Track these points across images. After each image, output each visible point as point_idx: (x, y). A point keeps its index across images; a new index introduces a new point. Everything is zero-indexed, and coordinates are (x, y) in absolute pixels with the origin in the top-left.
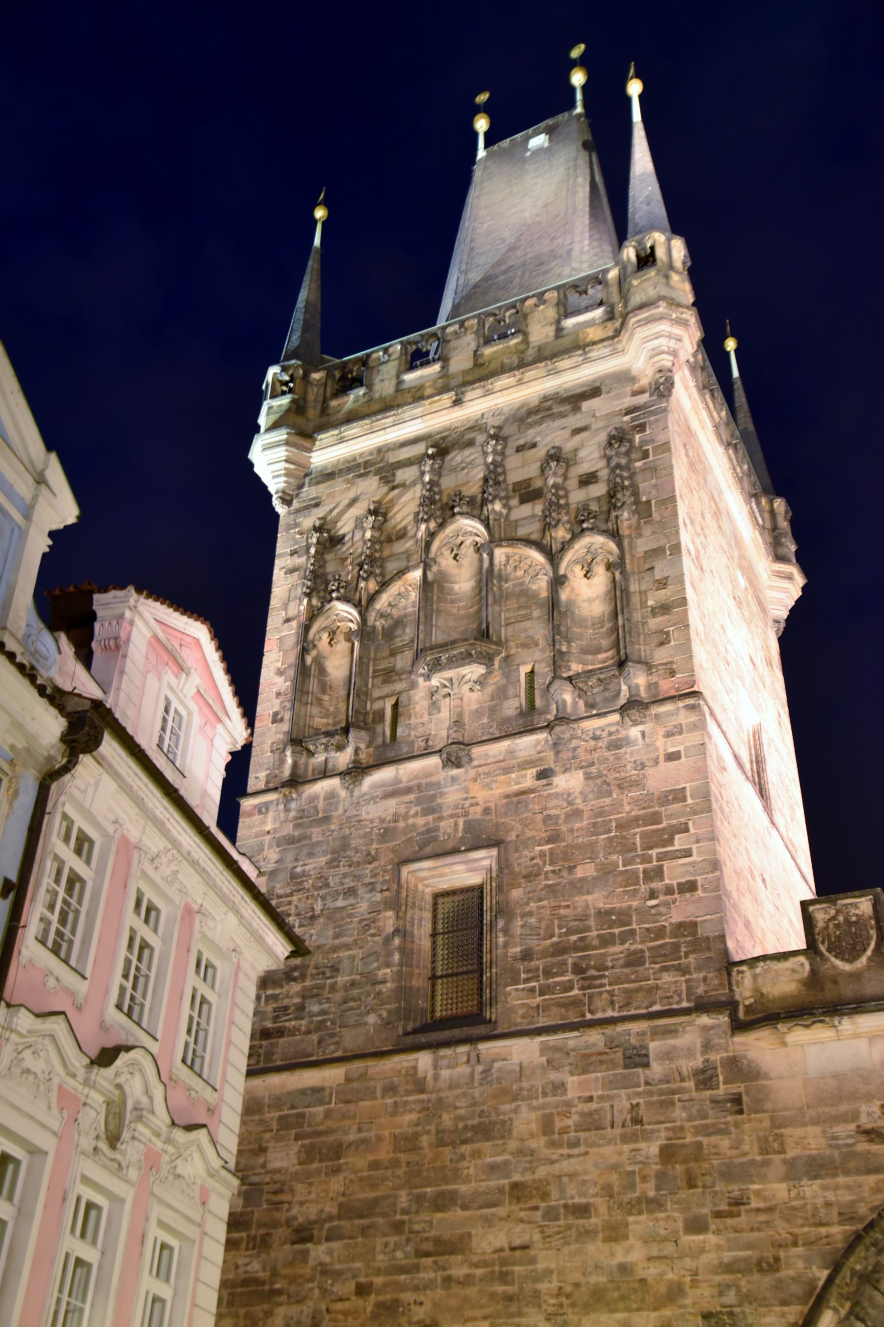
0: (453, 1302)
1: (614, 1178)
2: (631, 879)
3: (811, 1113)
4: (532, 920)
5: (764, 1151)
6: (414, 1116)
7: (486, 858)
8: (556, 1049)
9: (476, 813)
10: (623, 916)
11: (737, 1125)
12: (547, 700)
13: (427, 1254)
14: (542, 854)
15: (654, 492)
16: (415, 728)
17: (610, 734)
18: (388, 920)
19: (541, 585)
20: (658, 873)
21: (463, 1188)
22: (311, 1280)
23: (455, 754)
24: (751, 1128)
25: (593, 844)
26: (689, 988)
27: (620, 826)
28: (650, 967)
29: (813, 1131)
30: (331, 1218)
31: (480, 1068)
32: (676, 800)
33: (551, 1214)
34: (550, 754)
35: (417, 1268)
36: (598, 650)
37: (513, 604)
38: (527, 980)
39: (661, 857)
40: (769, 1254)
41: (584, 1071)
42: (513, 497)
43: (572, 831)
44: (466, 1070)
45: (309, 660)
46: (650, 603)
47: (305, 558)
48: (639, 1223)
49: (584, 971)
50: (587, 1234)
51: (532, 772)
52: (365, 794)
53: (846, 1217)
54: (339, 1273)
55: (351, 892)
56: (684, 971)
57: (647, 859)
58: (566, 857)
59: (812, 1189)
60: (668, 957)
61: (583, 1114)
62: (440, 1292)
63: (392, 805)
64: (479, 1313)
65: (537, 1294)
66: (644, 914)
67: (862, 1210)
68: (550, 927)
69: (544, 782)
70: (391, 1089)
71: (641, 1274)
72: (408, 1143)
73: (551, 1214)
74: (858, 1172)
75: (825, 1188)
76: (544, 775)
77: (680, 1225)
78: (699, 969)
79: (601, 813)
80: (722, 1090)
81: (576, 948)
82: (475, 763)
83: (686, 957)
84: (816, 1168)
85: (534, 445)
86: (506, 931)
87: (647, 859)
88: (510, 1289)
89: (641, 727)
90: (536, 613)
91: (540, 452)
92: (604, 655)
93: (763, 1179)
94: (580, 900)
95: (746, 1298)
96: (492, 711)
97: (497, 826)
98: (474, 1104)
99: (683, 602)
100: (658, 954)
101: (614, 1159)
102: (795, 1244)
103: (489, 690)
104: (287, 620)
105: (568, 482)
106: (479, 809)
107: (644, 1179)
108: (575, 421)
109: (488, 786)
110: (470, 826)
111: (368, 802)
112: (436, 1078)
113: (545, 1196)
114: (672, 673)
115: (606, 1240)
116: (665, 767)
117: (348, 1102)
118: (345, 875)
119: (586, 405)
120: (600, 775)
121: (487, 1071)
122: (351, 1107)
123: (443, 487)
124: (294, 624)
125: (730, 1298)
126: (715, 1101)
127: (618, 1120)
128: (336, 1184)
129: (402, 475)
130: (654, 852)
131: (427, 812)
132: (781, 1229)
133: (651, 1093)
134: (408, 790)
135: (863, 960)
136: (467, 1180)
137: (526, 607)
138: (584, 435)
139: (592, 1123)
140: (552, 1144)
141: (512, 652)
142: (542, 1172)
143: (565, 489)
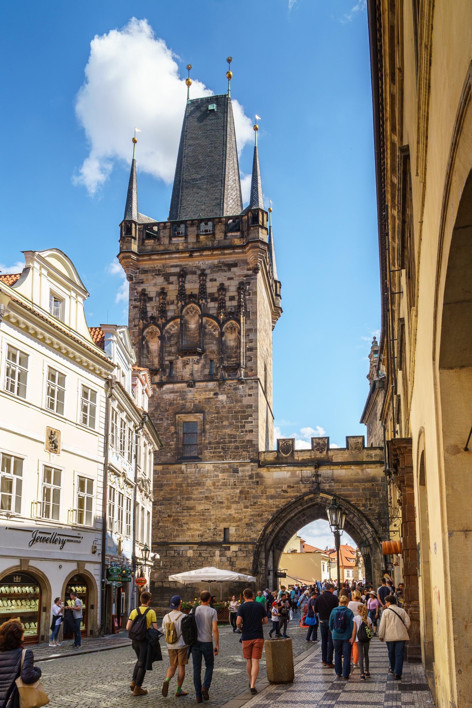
0: (191, 519)
1: (229, 496)
2: (237, 427)
3: (273, 486)
4: (212, 434)
5: (262, 493)
6: (181, 479)
7: (200, 416)
8: (217, 467)
9: (197, 402)
10: (235, 437)
11: (257, 487)
12: (217, 371)
13: (185, 510)
14: (215, 417)
15: (251, 309)
16: (178, 373)
17: (234, 385)
18: (172, 429)
19: (216, 333)
20: (244, 426)
21: (194, 496)
22: (157, 513)
23: (191, 384)
24: (260, 488)
25: (228, 416)
26: (249, 456)
27: (235, 412)
28: (240, 450)
29: (273, 490)
30: (161, 501)
31: (198, 470)
32: (250, 408)
33: (214, 503)
34: (218, 388)
35: (183, 512)
36: (232, 357)
37: (207, 337)
38: (210, 449)
39: (245, 422)
40: (261, 513)
41: (223, 473)
42: (209, 299)
43: (223, 412)
44: (195, 470)
45: (144, 343)
46: (247, 347)
47: (139, 303)
48: (234, 506)
49: (224, 449)
50: (222, 508)
51: (212, 393)
52: (164, 391)
53: (277, 507)
54: (164, 512)
55: (161, 419)
56: (249, 452)
57: (241, 422)
58: (221, 418)
59: (271, 501)
60: (245, 448)
61: (222, 482)
62: (188, 518)
63: (172, 396)
64: (198, 522)
65: (211, 519)
66: (239, 437)
67: (280, 506)
68: (216, 437)
69: (216, 396)
70: (175, 472)
71: (234, 516)
72: (180, 485)
73: (214, 503)
74: (281, 498)
75: (273, 501)
76: (216, 394)
77: (243, 507)
78: (252, 452)
79: (230, 408)
80: (254, 480)
81: (223, 443)
82: (196, 387)
83: (249, 448)
84: (272, 497)
85: (215, 280)
86: (204, 436)
87: (241, 422)
88: (204, 518)
89: (242, 385)
90: (215, 342)
91: (217, 284)
92: (233, 359)
93: (261, 499)
94: (224, 431)
95: (255, 521)
96: (202, 371)
97: (203, 407)
98: (196, 478)
99: (256, 348)
100: (243, 447)
101: (229, 493)
102: (266, 511)
103: (200, 365)
104: (135, 326)
105: (226, 298)
106: (197, 401)
107: (236, 497)
108: (229, 274)
109: (200, 395)
110: (195, 405)
111: (165, 393)
112: (186, 471)
113: (213, 499)
114: (252, 370)
115: (226, 509)
116: (248, 398)
117: (164, 474)
118: (159, 414)
119: (233, 269)
120: (231, 397)
121: (200, 470)
122: (164, 476)
123: (186, 288)
124: (137, 327)
125: (252, 521)
126: (253, 482)
127: (231, 484)
128: (162, 493)
129: (173, 279)
130: (243, 421)
131: (183, 399)
132: (264, 508)
133: (238, 479)
134: (177, 392)
135: (289, 454)
136: (195, 495)
137: (212, 340)
138: (232, 281)
139: (225, 484)
140: (215, 488)
141: (208, 353)
142: (212, 494)
143: (225, 300)
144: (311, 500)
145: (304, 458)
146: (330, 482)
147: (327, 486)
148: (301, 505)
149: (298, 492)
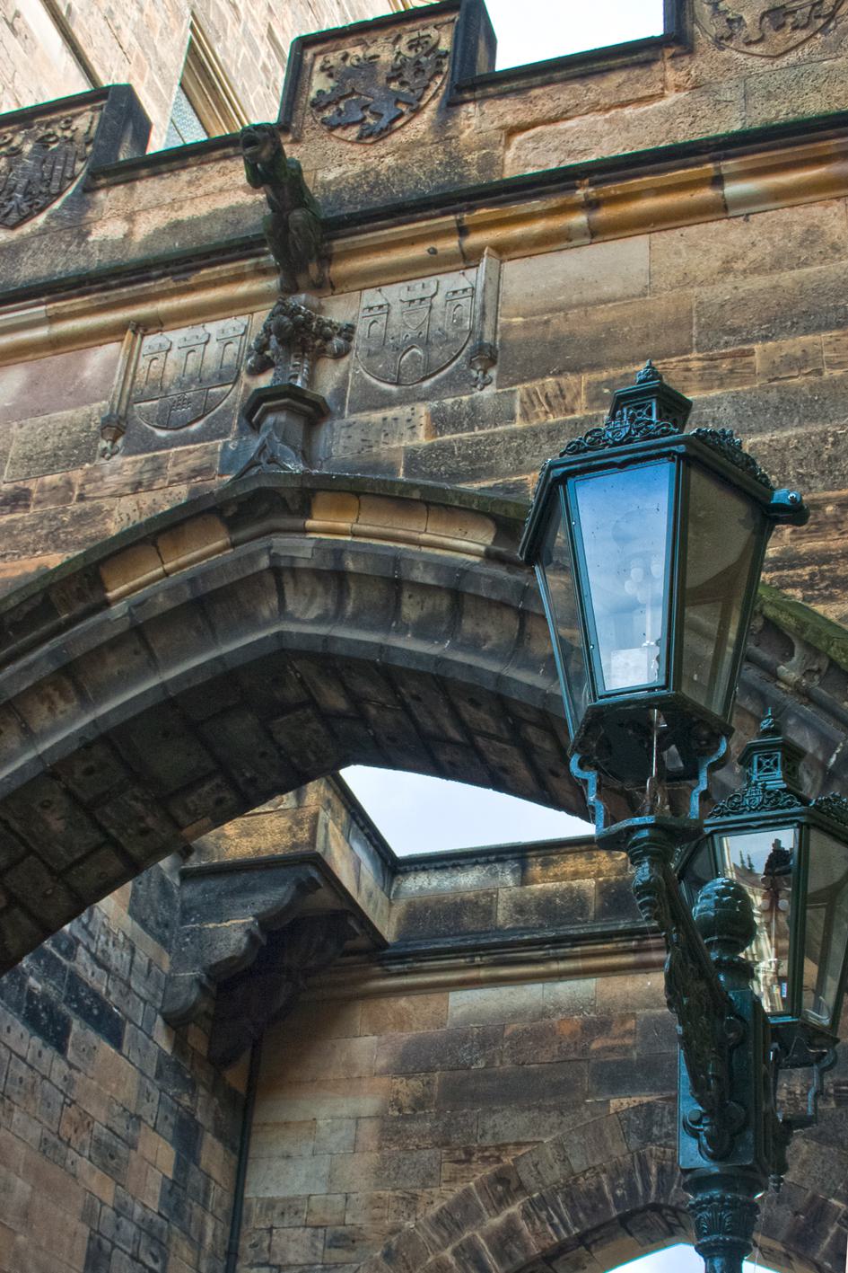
135: (40, 220)
144: (205, 606)
145: (186, 214)
146: (457, 383)
147: (406, 432)
148: (72, 677)
149: (54, 540)
